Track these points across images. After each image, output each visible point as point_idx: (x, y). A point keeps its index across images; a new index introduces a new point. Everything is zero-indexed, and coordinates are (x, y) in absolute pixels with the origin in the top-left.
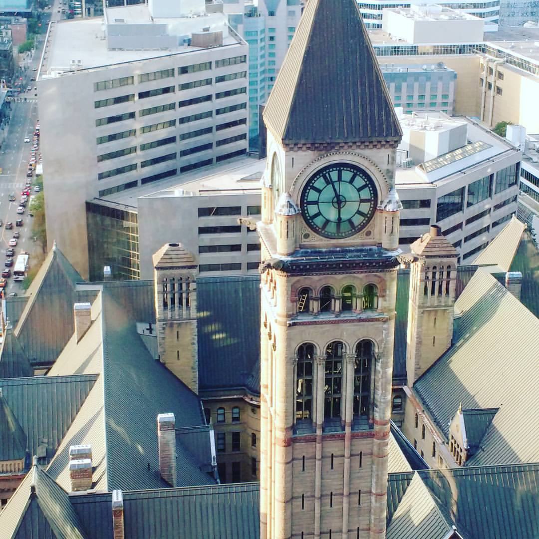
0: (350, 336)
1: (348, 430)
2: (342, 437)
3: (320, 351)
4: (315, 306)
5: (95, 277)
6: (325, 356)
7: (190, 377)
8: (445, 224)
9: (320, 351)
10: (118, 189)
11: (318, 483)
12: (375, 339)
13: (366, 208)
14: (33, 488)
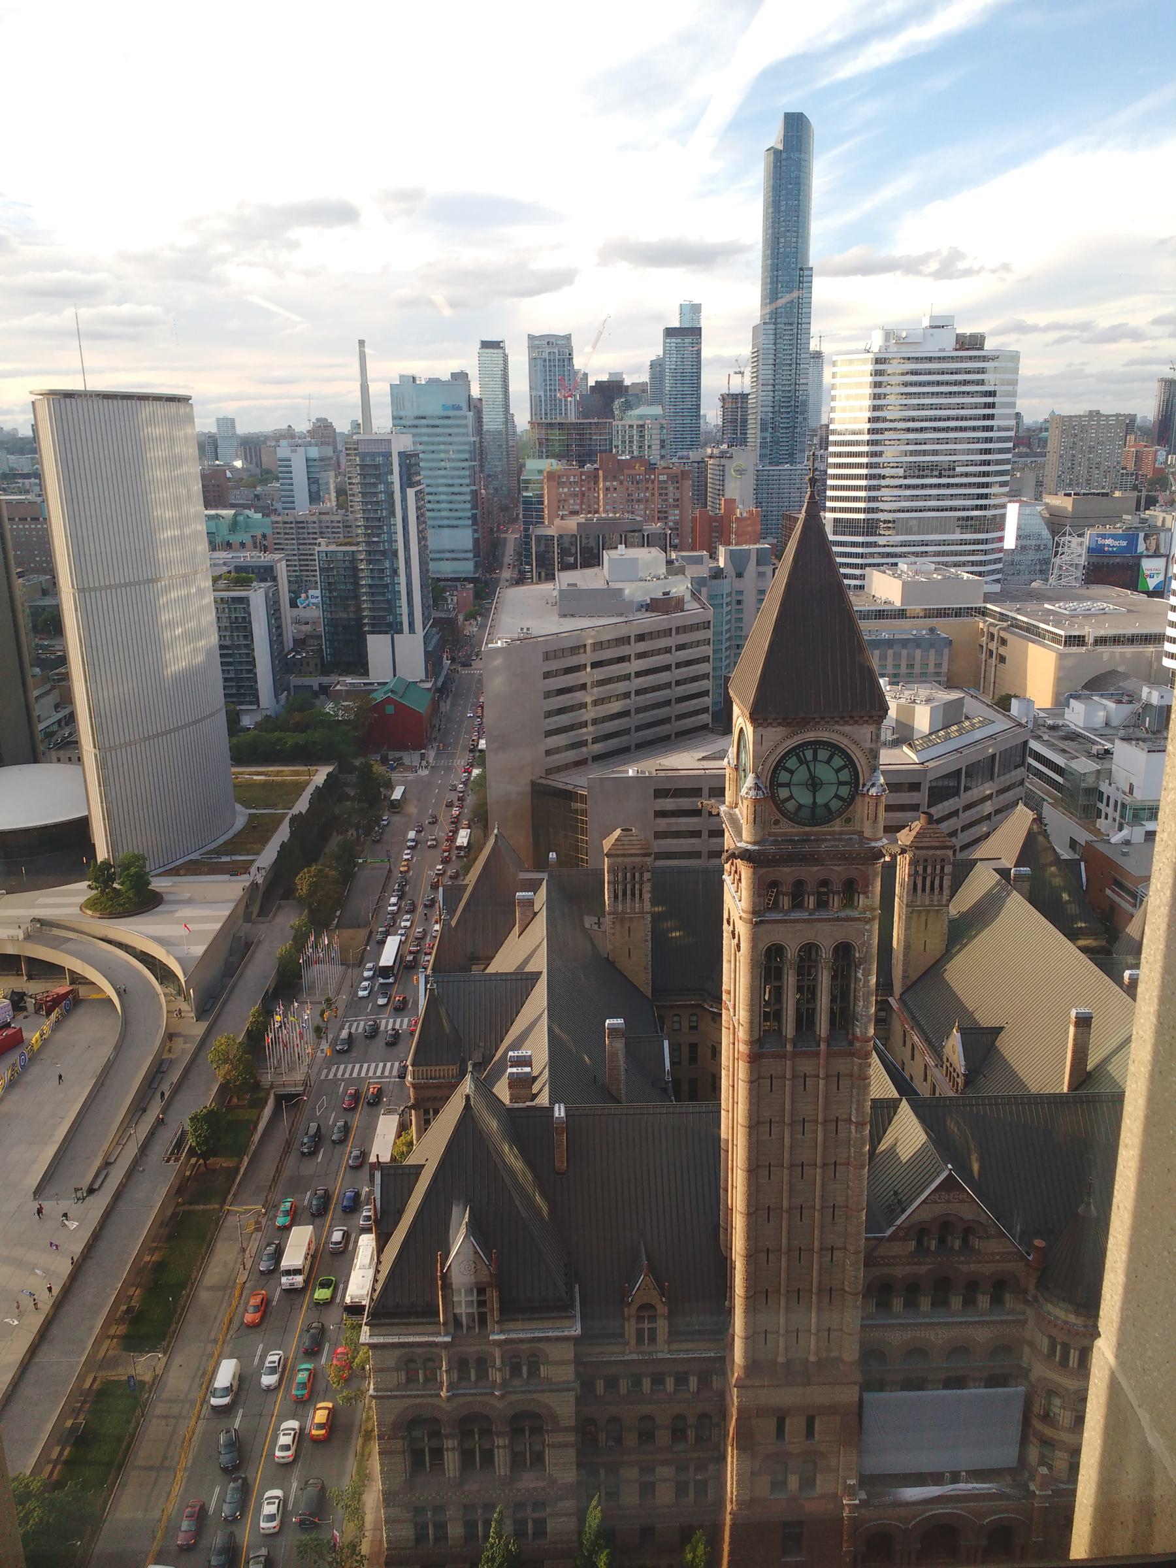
5: (540, 864)
7: (643, 979)
8: (937, 811)
10: (567, 767)
14: (468, 1097)
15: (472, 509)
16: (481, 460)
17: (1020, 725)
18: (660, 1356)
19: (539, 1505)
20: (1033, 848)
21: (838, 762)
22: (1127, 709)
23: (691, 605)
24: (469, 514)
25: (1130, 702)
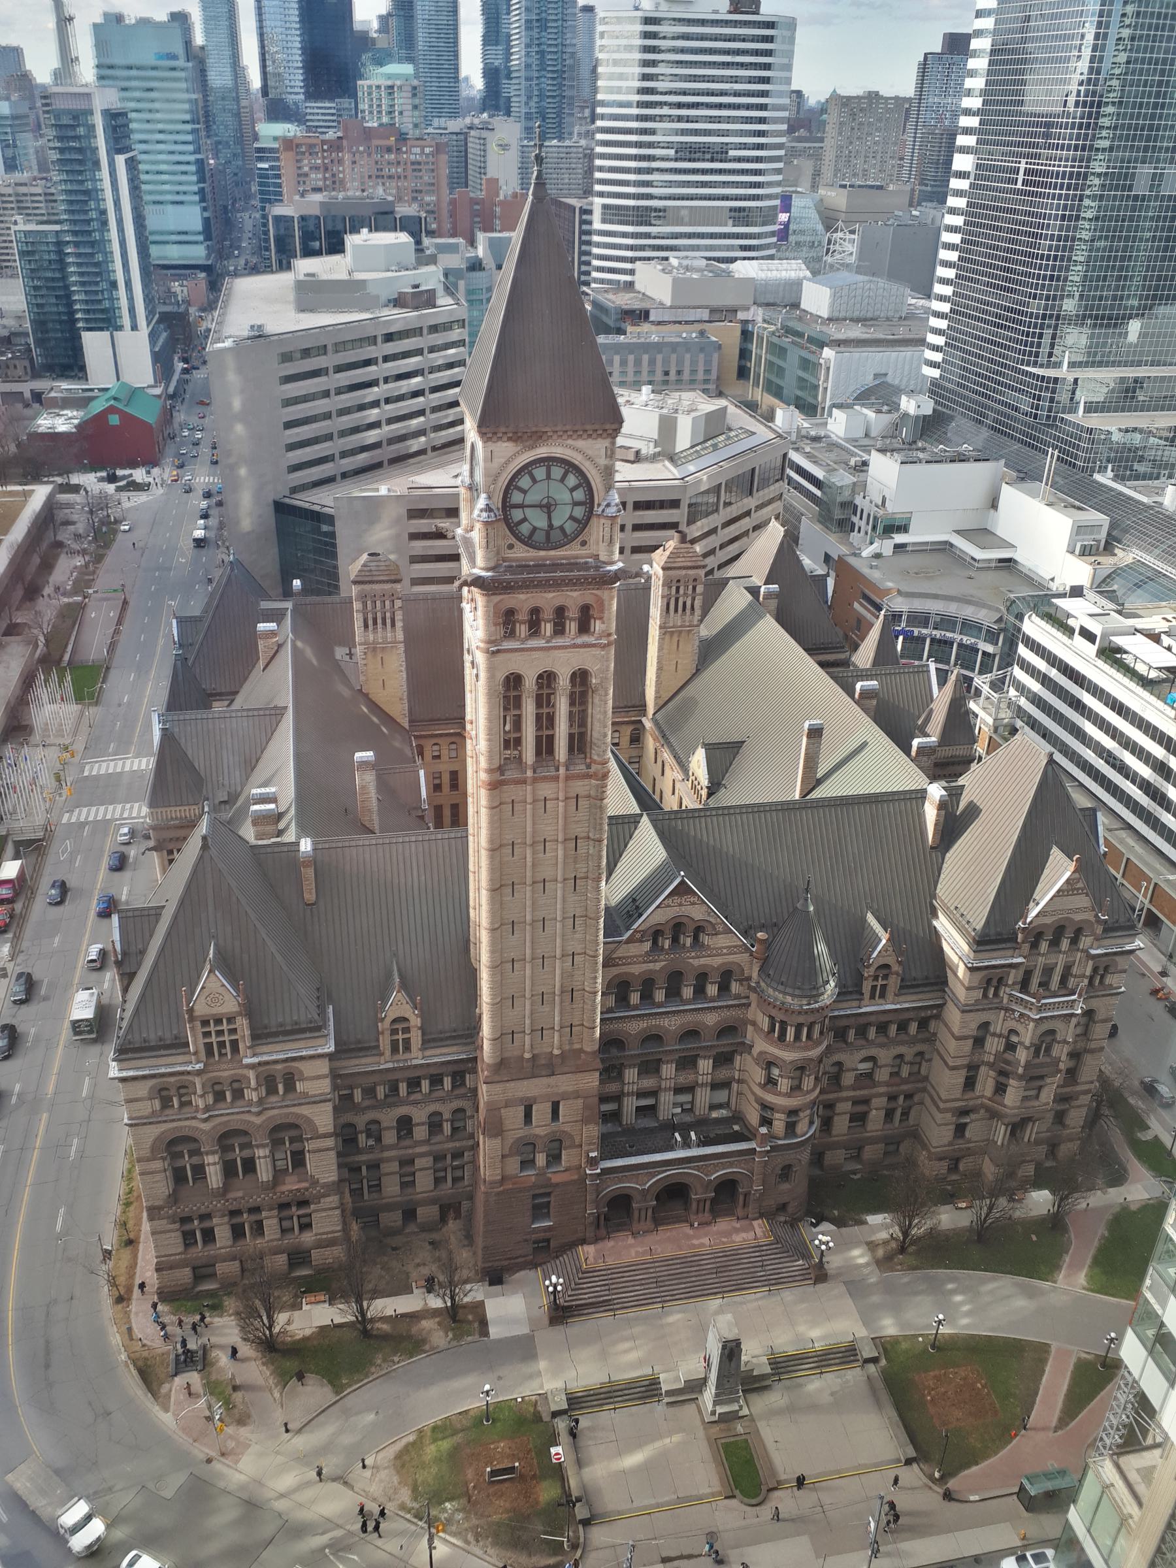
0: (564, 665)
1: (562, 770)
3: (530, 683)
4: (522, 630)
6: (535, 688)
8: (695, 531)
9: (530, 683)
11: (529, 829)
12: (593, 667)
15: (199, 182)
16: (207, 122)
17: (780, 436)
18: (415, 1062)
19: (303, 1203)
20: (785, 563)
22: (886, 419)
23: (444, 301)
24: (195, 188)
25: (889, 412)
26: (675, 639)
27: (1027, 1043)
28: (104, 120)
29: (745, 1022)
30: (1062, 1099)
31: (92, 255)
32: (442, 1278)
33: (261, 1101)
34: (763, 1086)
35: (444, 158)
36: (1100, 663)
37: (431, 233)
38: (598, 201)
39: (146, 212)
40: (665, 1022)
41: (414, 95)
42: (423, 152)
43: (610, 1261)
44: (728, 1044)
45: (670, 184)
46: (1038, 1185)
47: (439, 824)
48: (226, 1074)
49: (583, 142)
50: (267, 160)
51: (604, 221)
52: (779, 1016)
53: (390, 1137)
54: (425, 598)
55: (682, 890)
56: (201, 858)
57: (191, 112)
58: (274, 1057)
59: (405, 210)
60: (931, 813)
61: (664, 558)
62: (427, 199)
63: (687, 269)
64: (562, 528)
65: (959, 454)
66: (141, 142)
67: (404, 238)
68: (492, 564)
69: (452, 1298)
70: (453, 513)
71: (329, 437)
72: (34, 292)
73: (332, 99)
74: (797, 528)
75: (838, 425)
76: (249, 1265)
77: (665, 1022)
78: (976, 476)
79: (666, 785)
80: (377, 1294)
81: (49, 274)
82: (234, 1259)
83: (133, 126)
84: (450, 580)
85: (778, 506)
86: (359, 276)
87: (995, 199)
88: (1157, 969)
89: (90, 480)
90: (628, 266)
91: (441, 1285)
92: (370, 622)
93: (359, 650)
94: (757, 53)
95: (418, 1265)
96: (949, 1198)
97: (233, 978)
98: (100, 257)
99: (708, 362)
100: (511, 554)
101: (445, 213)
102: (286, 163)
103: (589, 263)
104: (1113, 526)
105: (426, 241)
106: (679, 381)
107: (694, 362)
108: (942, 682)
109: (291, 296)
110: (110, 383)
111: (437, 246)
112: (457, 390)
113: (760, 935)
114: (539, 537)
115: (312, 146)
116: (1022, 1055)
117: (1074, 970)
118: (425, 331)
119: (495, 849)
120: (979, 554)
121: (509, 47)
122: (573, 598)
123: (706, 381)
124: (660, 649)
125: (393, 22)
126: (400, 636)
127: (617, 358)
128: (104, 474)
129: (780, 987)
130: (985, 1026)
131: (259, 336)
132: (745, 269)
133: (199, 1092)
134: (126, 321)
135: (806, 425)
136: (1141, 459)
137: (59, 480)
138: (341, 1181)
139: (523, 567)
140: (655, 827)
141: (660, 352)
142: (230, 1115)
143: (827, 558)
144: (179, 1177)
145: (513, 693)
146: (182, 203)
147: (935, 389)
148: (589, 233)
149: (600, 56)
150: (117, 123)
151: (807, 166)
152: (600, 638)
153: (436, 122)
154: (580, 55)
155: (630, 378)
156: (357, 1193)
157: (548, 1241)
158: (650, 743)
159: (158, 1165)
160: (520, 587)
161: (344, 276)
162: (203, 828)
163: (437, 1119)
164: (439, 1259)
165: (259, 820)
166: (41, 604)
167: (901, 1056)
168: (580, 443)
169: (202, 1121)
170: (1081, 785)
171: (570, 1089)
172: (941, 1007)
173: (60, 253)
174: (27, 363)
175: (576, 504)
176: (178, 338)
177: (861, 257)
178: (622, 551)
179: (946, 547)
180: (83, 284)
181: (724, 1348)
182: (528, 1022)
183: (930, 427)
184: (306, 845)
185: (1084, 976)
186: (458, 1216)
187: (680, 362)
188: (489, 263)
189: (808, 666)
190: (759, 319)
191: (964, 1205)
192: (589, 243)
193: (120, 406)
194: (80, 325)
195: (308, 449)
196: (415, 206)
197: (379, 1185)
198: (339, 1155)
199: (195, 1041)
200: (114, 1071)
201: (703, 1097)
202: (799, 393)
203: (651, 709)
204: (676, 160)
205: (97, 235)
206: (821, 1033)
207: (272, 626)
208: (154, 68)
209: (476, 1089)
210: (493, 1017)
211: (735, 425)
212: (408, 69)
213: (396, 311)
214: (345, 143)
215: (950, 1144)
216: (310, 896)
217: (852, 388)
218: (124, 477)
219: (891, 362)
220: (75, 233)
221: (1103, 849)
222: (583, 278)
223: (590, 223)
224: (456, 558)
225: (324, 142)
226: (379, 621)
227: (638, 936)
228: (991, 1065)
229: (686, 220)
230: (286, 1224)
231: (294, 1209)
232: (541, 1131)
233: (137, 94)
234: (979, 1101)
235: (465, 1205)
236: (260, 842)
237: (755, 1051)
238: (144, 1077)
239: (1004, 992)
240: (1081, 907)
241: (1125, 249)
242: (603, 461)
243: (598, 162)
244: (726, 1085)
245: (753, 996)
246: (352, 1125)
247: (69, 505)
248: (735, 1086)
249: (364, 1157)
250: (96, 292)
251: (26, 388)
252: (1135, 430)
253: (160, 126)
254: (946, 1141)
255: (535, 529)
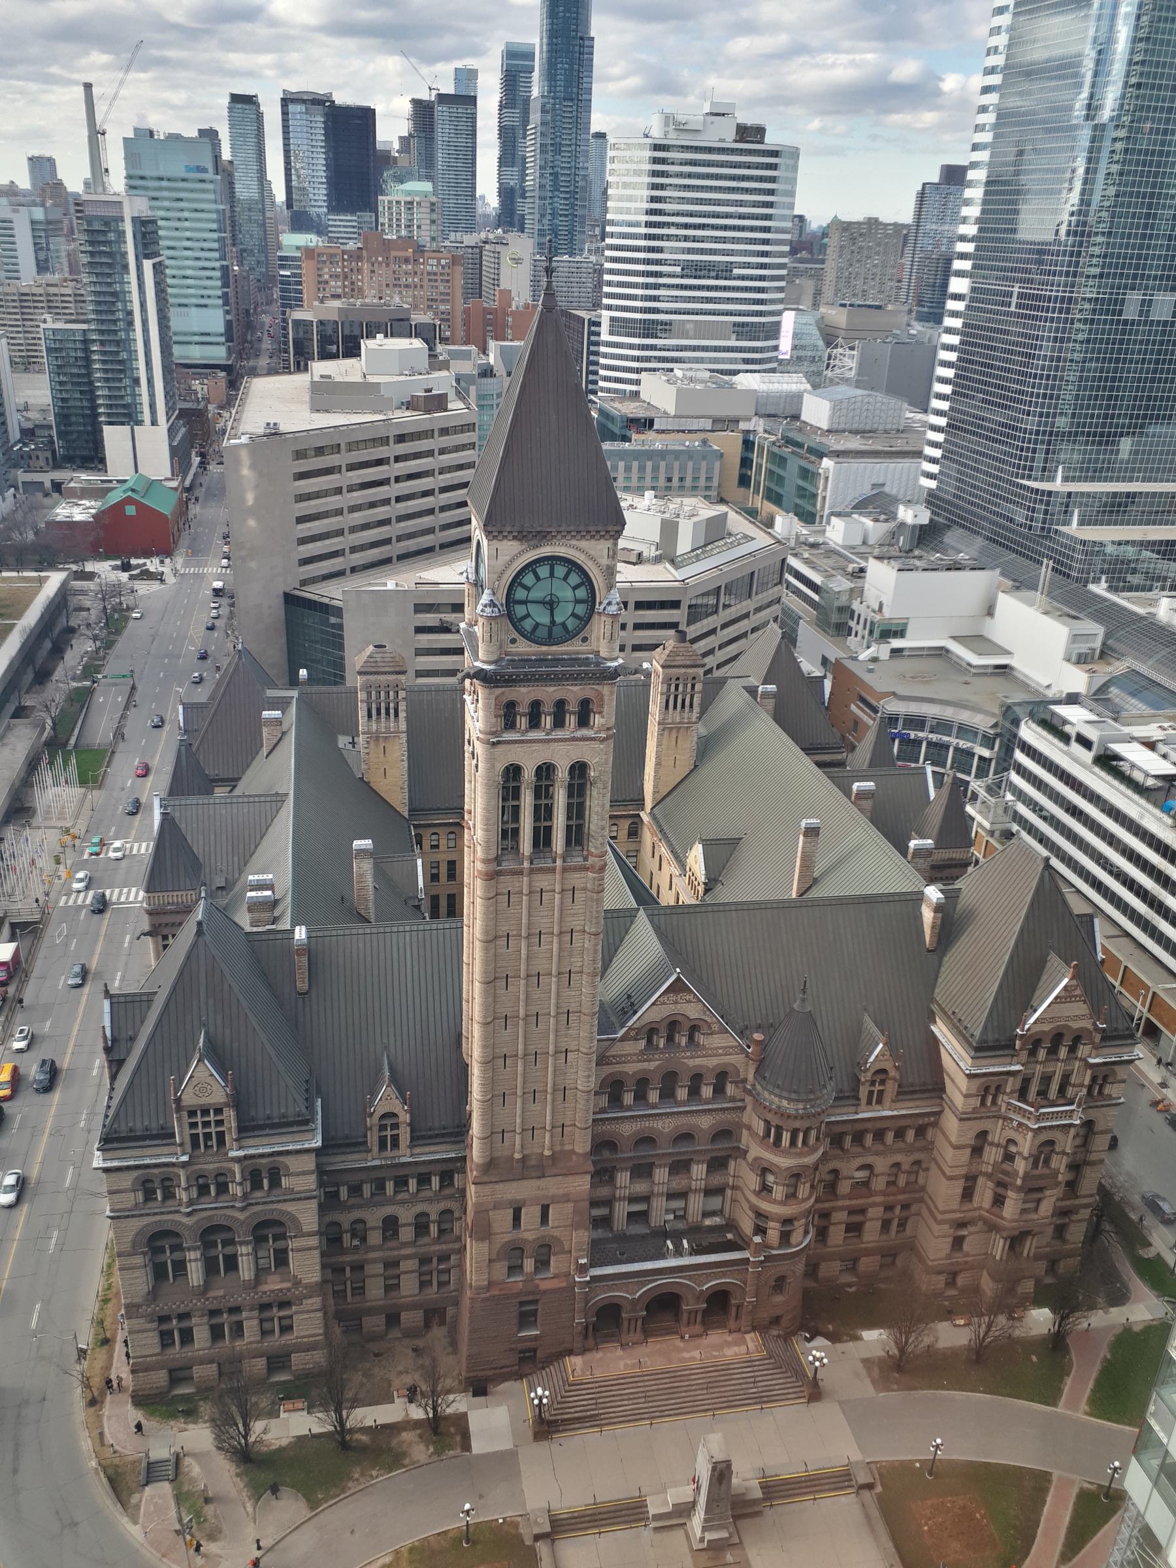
0: (562, 758)
1: (559, 862)
2: (553, 870)
3: (528, 775)
4: (522, 722)
8: (692, 631)
9: (528, 775)
13: (581, 610)
17: (779, 542)
18: (403, 1160)
20: (783, 666)
21: (574, 579)
25: (886, 521)
26: (674, 735)
27: (1026, 1154)
28: (134, 226)
29: (740, 1126)
30: (1063, 1213)
31: (117, 353)
32: (424, 1387)
33: (245, 1196)
34: (758, 1194)
35: (459, 269)
36: (1097, 770)
37: (444, 340)
38: (606, 315)
39: (171, 314)
40: (659, 1125)
41: (433, 211)
42: (439, 263)
43: (598, 1373)
44: (723, 1149)
45: (676, 299)
46: (1039, 1304)
47: (435, 914)
48: (211, 1166)
49: (593, 258)
50: (290, 267)
51: (611, 333)
52: (775, 1121)
53: (375, 1238)
54: (429, 689)
55: (677, 987)
56: (195, 945)
57: (218, 221)
58: (261, 1151)
59: (418, 318)
60: (928, 915)
61: (664, 657)
62: (442, 307)
63: (691, 380)
64: (563, 624)
65: (956, 562)
66: (169, 248)
67: (417, 343)
68: (495, 658)
69: (434, 1409)
70: (458, 608)
71: (340, 533)
72: (58, 387)
73: (353, 213)
74: (795, 631)
75: (836, 532)
76: (229, 1367)
77: (659, 1125)
78: (971, 585)
79: (662, 879)
80: (356, 1403)
81: (75, 371)
82: (212, 1362)
83: (161, 233)
84: (452, 673)
85: (776, 609)
86: (371, 379)
87: (989, 320)
88: (1157, 1079)
89: (105, 570)
90: (634, 376)
91: (423, 1395)
92: (374, 712)
93: (361, 740)
94: (761, 179)
95: (400, 1373)
96: (948, 1314)
97: (222, 1068)
98: (124, 355)
99: (710, 470)
100: (513, 648)
101: (459, 321)
102: (308, 270)
103: (596, 373)
104: (1107, 636)
105: (440, 348)
106: (681, 488)
107: (696, 470)
108: (939, 783)
109: (307, 398)
110: (128, 475)
111: (450, 352)
112: (465, 491)
113: (758, 1036)
114: (542, 633)
115: (332, 256)
116: (1021, 1166)
117: (1073, 1080)
118: (436, 434)
119: (491, 940)
120: (975, 660)
121: (524, 169)
122: (574, 693)
123: (708, 488)
124: (659, 744)
125: (414, 143)
126: (403, 726)
127: (621, 464)
128: (119, 563)
129: (777, 1091)
130: (983, 1135)
131: (273, 433)
132: (749, 381)
133: (183, 1184)
134: (147, 416)
135: (805, 532)
136: (1134, 571)
137: (74, 567)
138: (324, 1282)
139: (525, 661)
140: (651, 922)
141: (663, 459)
142: (212, 1208)
143: (825, 661)
144: (159, 1272)
145: (511, 784)
146: (206, 306)
147: (932, 500)
148: (597, 344)
149: (610, 179)
150: (147, 232)
151: (809, 285)
152: (599, 732)
153: (452, 236)
154: (592, 177)
155: (634, 482)
156: (339, 1295)
157: (535, 1350)
158: (648, 837)
159: (138, 1260)
160: (522, 681)
161: (360, 380)
162: (199, 914)
163: (424, 1220)
164: (422, 1367)
165: (254, 906)
166: (50, 687)
167: (897, 1165)
168: (584, 544)
169: (183, 1212)
170: (1078, 891)
171: (561, 1192)
172: (939, 1113)
173: (86, 350)
174: (49, 454)
175: (578, 601)
176: (196, 434)
177: (859, 374)
178: (622, 648)
179: (941, 653)
180: (107, 380)
181: (714, 1469)
182: (518, 1120)
183: (926, 536)
184: (300, 933)
185: (1082, 1085)
186: (442, 1323)
187: (683, 469)
188: (500, 370)
189: (805, 765)
190: (760, 429)
191: (962, 1322)
192: (597, 353)
193: (134, 496)
194: (102, 419)
195: (319, 544)
196: (430, 314)
197: (363, 1288)
198: (323, 1254)
199: (181, 1133)
200: (98, 1161)
201: (696, 1204)
202: (799, 501)
203: (649, 804)
204: (682, 277)
205: (122, 335)
206: (818, 1139)
207: (277, 714)
208: (183, 180)
209: (464, 1190)
210: (484, 1114)
211: (734, 531)
212: (427, 186)
213: (408, 413)
214: (365, 253)
215: (948, 1257)
216: (303, 986)
217: (849, 498)
218: (138, 566)
219: (891, 474)
220: (101, 332)
221: (1100, 956)
222: (590, 387)
223: (599, 334)
224: (460, 651)
225: (344, 252)
226: (383, 711)
227: (632, 1033)
228: (989, 1176)
229: (691, 333)
230: (267, 1326)
231: (275, 1310)
232: (529, 1236)
233: (166, 204)
234: (977, 1214)
235: (450, 1311)
236: (255, 929)
237: (750, 1156)
238: (128, 1168)
239: (1002, 1100)
240: (1078, 1015)
241: (1116, 370)
242: (605, 561)
243: (606, 277)
244: (719, 1191)
245: (749, 1100)
246: (338, 1224)
247: (83, 592)
248: (729, 1192)
249: (348, 1258)
250: (119, 388)
251: (46, 478)
252: (1127, 543)
253: (188, 234)
254: (943, 1254)
255: (537, 625)
